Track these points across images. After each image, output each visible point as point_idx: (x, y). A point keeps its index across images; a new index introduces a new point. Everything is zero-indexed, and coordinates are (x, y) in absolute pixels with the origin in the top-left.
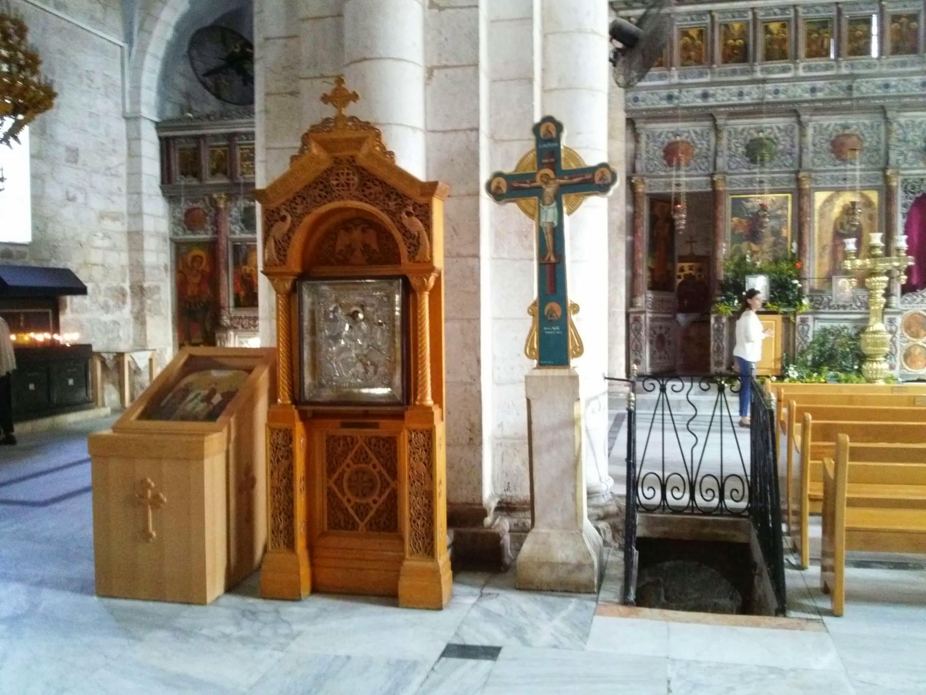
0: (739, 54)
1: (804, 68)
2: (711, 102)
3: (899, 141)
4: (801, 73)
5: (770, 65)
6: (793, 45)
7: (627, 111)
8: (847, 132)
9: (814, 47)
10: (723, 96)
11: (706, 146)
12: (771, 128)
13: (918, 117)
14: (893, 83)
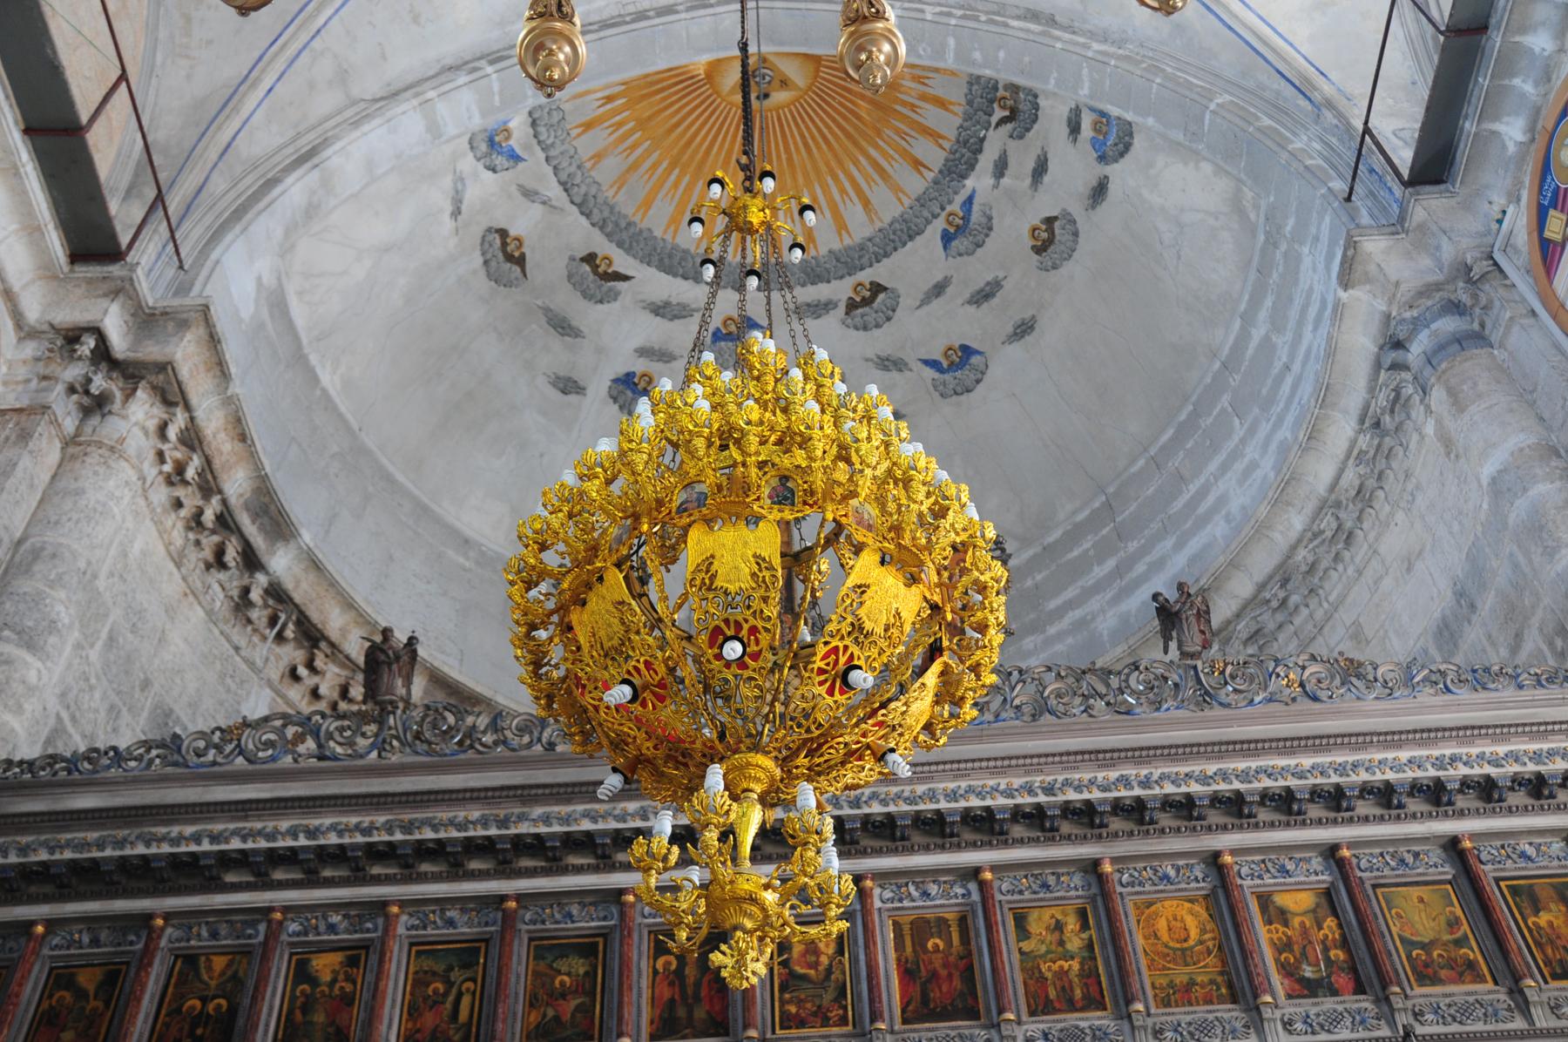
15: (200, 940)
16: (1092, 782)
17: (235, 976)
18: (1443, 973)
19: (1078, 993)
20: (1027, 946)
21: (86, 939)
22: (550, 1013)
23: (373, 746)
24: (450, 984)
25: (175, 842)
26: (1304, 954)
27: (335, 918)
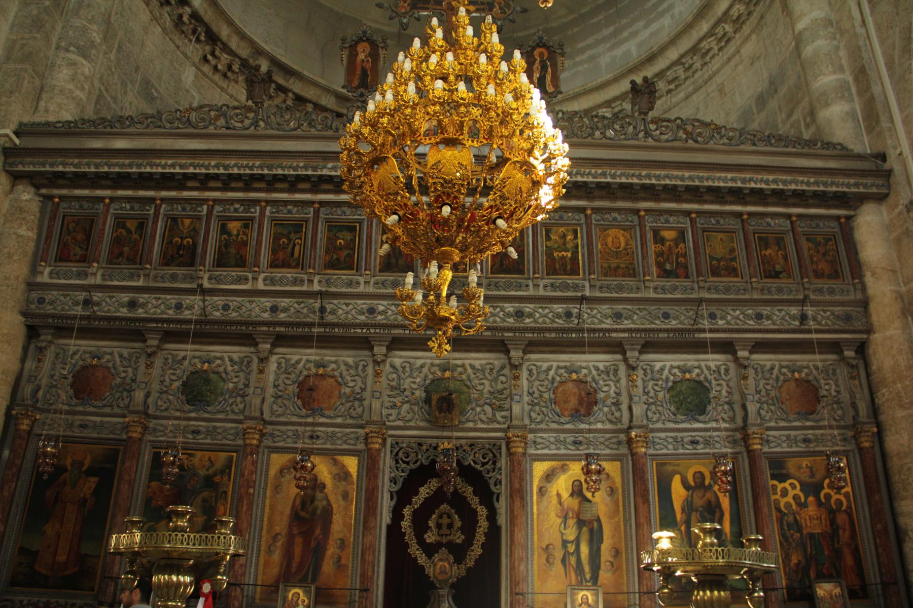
0: (182, 254)
1: (265, 280)
2: (140, 313)
3: (392, 388)
4: (261, 286)
5: (222, 272)
6: (253, 252)
7: (24, 314)
8: (321, 371)
9: (281, 255)
10: (155, 307)
11: (131, 375)
12: (222, 358)
13: (418, 358)
14: (381, 308)
15: (178, 210)
16: (589, 174)
17: (194, 229)
18: (723, 272)
19: (569, 267)
20: (549, 244)
21: (128, 207)
22: (335, 256)
23: (252, 124)
24: (290, 240)
25: (164, 167)
26: (668, 259)
27: (237, 206)
